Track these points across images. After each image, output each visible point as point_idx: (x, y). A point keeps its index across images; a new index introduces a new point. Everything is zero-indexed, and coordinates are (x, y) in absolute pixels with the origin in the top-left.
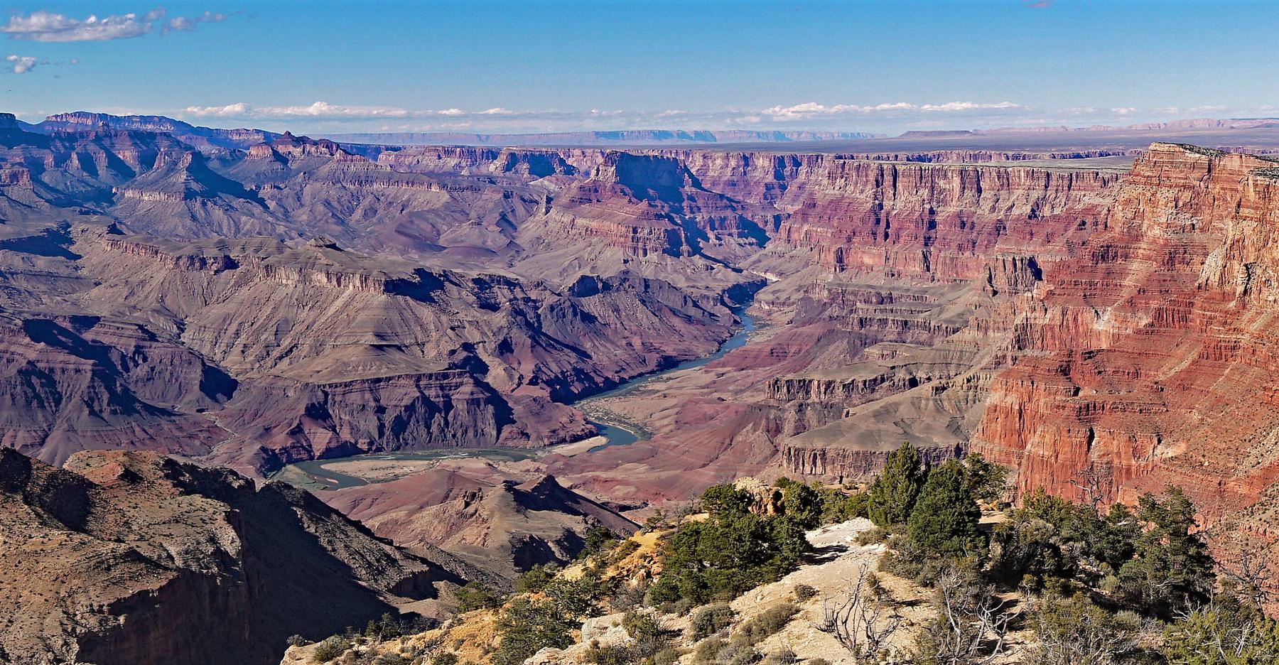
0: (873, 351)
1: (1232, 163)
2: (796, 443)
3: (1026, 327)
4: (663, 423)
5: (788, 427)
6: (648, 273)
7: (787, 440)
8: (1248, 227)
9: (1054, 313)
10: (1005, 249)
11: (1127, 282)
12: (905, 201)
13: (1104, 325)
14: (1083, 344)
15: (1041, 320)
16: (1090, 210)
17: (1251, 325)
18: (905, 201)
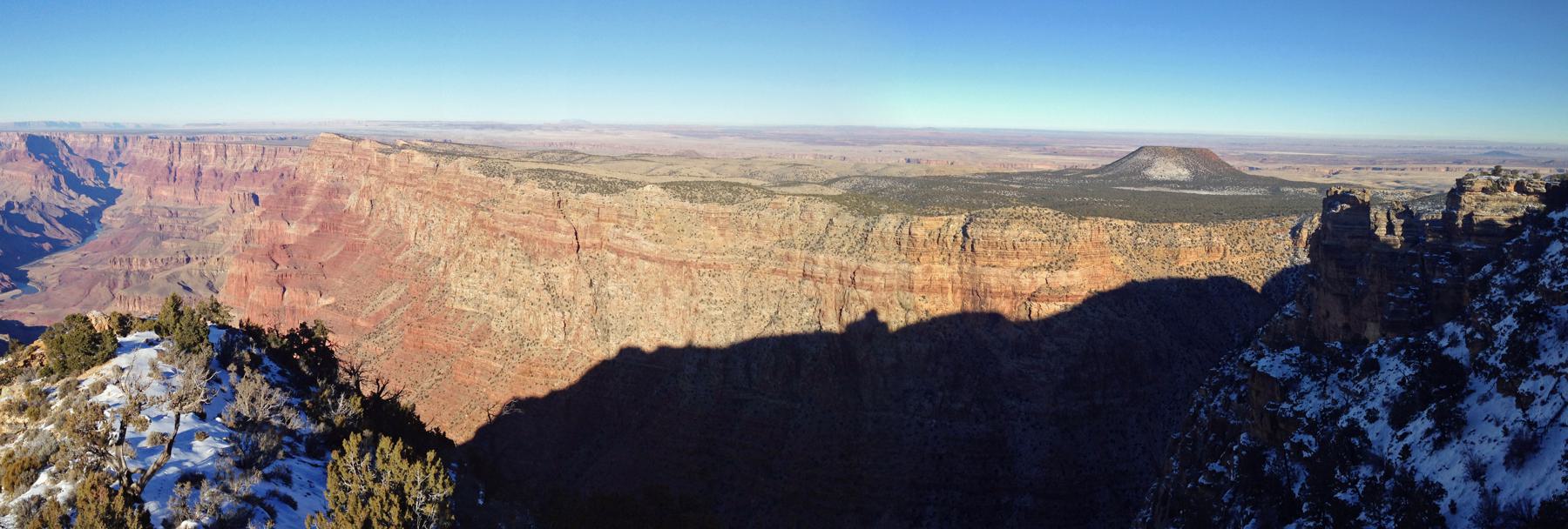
0: (167, 244)
1: (366, 145)
2: (123, 293)
3: (251, 231)
4: (52, 281)
5: (120, 284)
6: (43, 199)
7: (119, 292)
8: (373, 180)
9: (266, 223)
10: (238, 189)
11: (306, 208)
12: (185, 162)
13: (292, 232)
14: (281, 241)
15: (258, 227)
16: (284, 168)
17: (372, 234)
18: (185, 162)
